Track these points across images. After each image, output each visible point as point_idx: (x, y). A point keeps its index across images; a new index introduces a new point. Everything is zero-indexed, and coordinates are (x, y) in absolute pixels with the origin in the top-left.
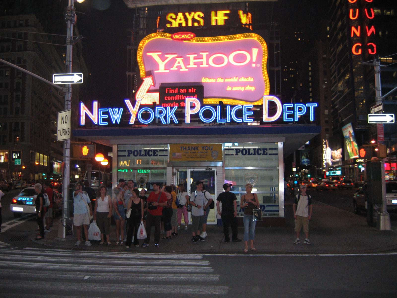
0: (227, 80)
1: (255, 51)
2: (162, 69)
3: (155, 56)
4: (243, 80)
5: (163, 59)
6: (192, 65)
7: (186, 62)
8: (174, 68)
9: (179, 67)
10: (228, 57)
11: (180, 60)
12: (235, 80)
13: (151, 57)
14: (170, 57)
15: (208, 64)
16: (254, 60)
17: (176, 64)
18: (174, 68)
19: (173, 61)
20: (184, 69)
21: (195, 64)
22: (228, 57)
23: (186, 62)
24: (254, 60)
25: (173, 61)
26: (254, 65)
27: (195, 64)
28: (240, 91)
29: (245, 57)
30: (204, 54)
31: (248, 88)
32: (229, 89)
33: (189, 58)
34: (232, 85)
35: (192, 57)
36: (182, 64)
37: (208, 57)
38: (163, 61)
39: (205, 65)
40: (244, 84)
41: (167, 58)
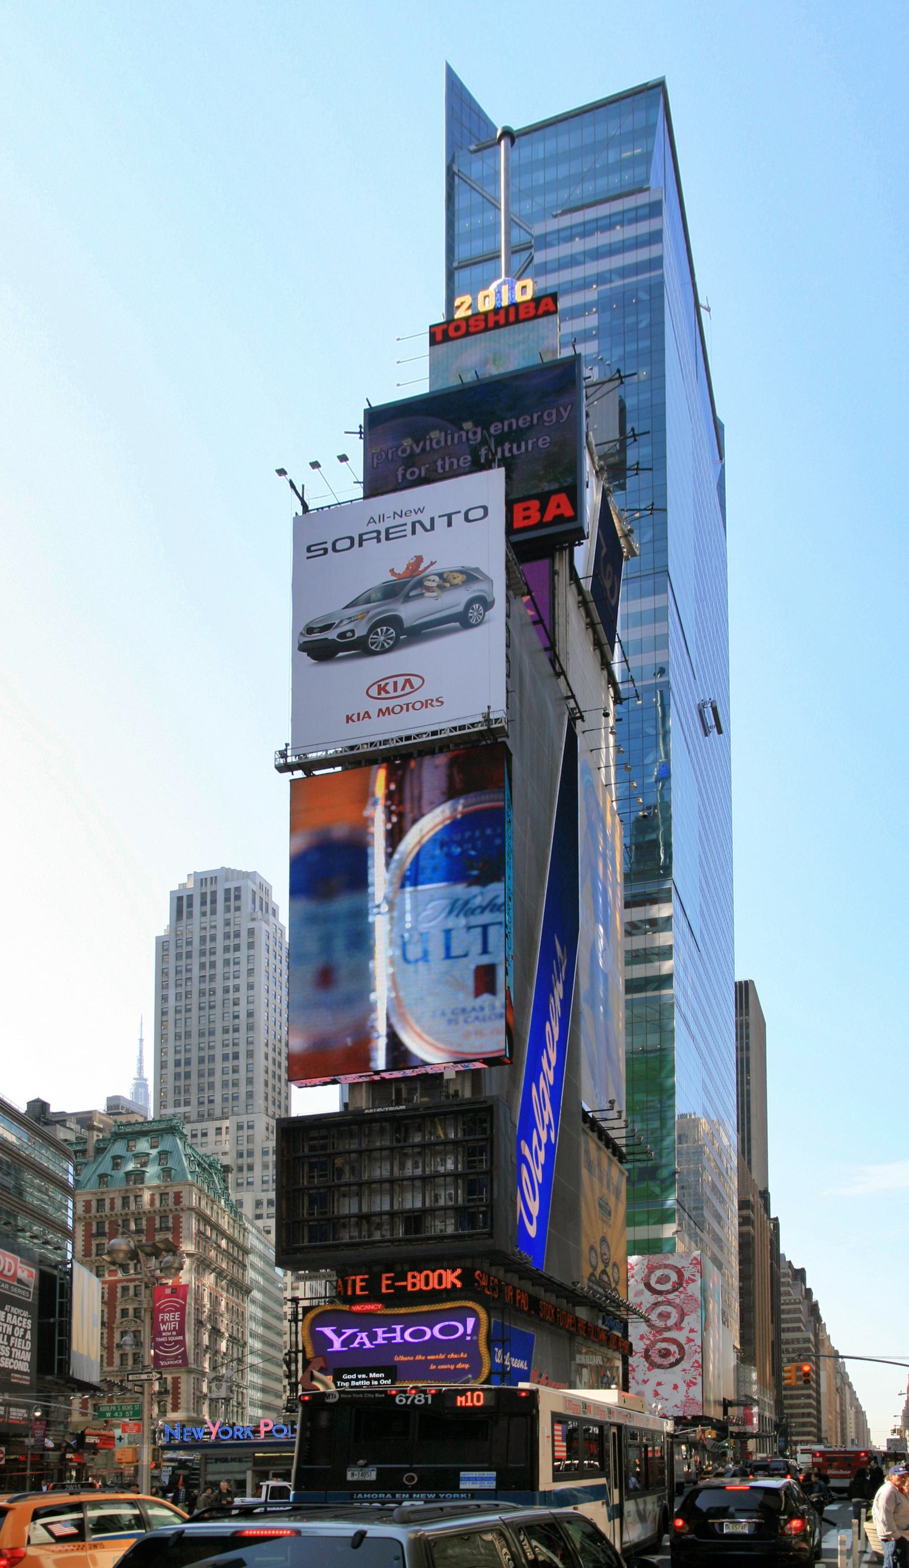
0: (429, 1357)
1: (471, 1322)
2: (337, 1345)
3: (328, 1331)
4: (452, 1356)
5: (339, 1334)
6: (380, 1341)
7: (372, 1337)
8: (355, 1345)
9: (363, 1344)
10: (431, 1329)
11: (364, 1334)
12: (442, 1356)
13: (322, 1332)
14: (349, 1332)
15: (402, 1337)
16: (469, 1331)
17: (358, 1340)
18: (355, 1345)
19: (354, 1336)
20: (368, 1345)
21: (384, 1339)
22: (431, 1329)
23: (372, 1337)
24: (469, 1331)
25: (354, 1336)
26: (468, 1338)
27: (384, 1339)
28: (449, 1369)
29: (456, 1329)
30: (398, 1328)
31: (459, 1366)
32: (433, 1367)
33: (376, 1332)
34: (437, 1362)
35: (380, 1331)
36: (366, 1340)
37: (403, 1331)
38: (339, 1337)
39: (398, 1340)
40: (455, 1361)
41: (345, 1333)
